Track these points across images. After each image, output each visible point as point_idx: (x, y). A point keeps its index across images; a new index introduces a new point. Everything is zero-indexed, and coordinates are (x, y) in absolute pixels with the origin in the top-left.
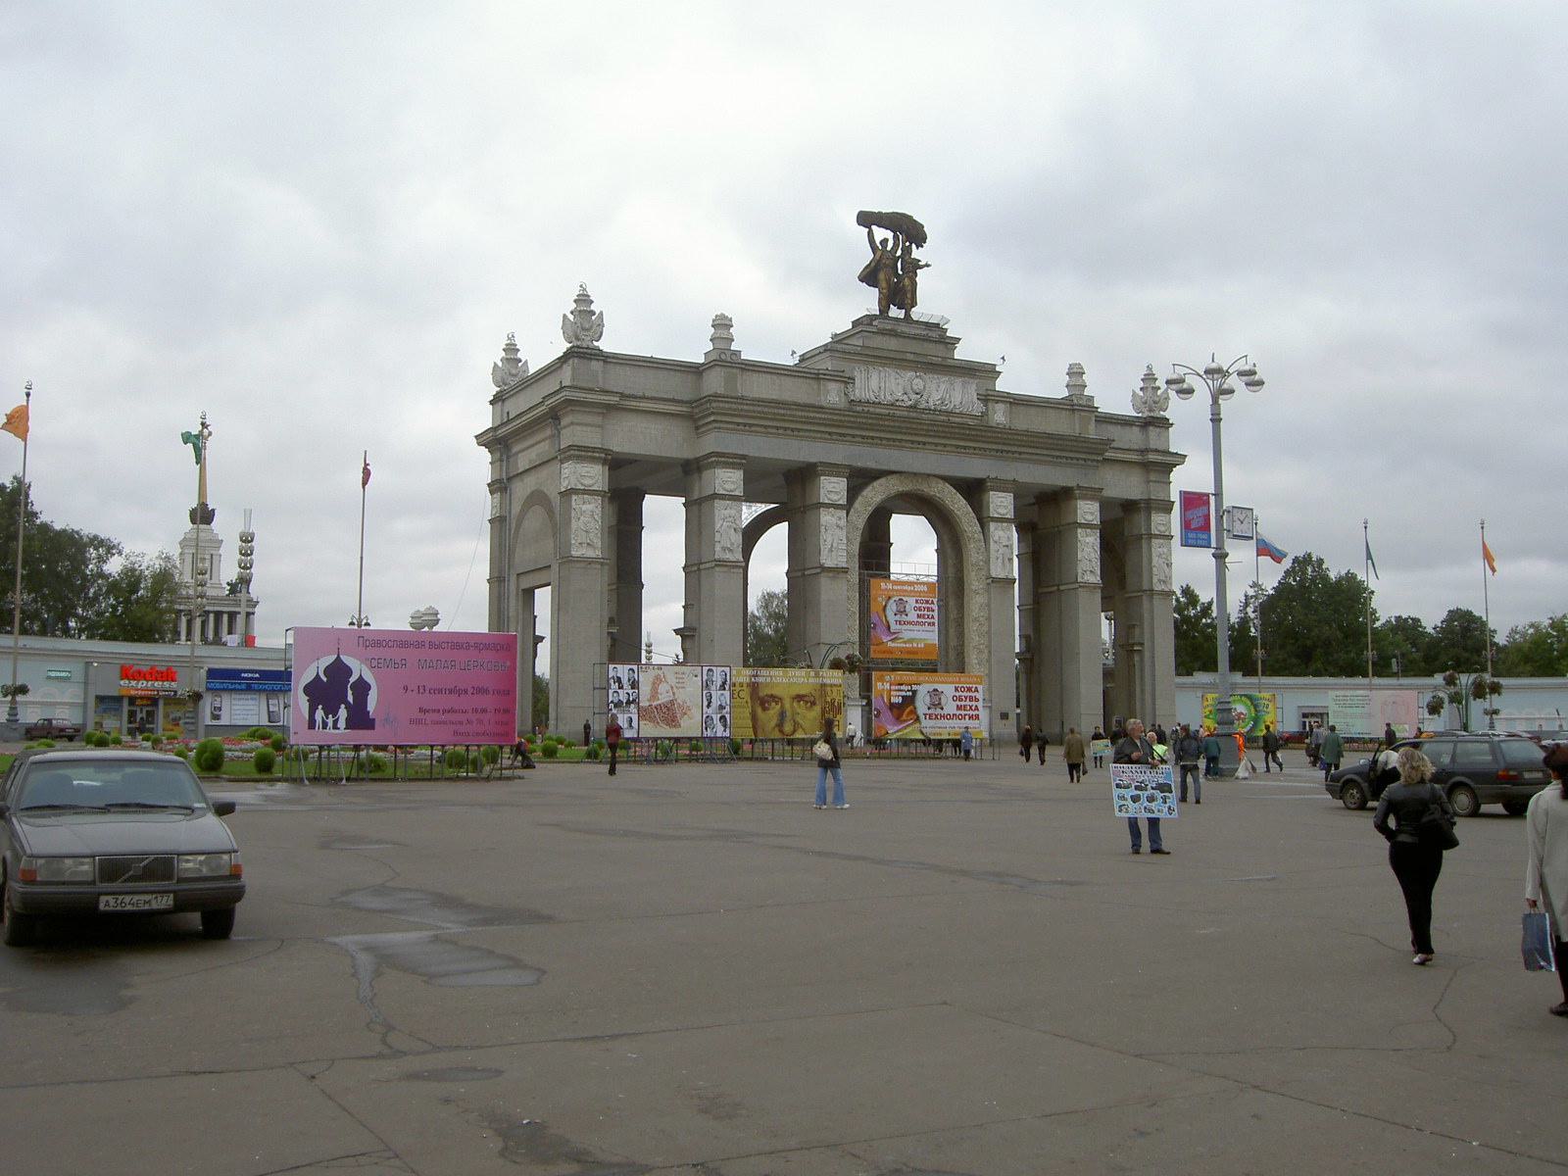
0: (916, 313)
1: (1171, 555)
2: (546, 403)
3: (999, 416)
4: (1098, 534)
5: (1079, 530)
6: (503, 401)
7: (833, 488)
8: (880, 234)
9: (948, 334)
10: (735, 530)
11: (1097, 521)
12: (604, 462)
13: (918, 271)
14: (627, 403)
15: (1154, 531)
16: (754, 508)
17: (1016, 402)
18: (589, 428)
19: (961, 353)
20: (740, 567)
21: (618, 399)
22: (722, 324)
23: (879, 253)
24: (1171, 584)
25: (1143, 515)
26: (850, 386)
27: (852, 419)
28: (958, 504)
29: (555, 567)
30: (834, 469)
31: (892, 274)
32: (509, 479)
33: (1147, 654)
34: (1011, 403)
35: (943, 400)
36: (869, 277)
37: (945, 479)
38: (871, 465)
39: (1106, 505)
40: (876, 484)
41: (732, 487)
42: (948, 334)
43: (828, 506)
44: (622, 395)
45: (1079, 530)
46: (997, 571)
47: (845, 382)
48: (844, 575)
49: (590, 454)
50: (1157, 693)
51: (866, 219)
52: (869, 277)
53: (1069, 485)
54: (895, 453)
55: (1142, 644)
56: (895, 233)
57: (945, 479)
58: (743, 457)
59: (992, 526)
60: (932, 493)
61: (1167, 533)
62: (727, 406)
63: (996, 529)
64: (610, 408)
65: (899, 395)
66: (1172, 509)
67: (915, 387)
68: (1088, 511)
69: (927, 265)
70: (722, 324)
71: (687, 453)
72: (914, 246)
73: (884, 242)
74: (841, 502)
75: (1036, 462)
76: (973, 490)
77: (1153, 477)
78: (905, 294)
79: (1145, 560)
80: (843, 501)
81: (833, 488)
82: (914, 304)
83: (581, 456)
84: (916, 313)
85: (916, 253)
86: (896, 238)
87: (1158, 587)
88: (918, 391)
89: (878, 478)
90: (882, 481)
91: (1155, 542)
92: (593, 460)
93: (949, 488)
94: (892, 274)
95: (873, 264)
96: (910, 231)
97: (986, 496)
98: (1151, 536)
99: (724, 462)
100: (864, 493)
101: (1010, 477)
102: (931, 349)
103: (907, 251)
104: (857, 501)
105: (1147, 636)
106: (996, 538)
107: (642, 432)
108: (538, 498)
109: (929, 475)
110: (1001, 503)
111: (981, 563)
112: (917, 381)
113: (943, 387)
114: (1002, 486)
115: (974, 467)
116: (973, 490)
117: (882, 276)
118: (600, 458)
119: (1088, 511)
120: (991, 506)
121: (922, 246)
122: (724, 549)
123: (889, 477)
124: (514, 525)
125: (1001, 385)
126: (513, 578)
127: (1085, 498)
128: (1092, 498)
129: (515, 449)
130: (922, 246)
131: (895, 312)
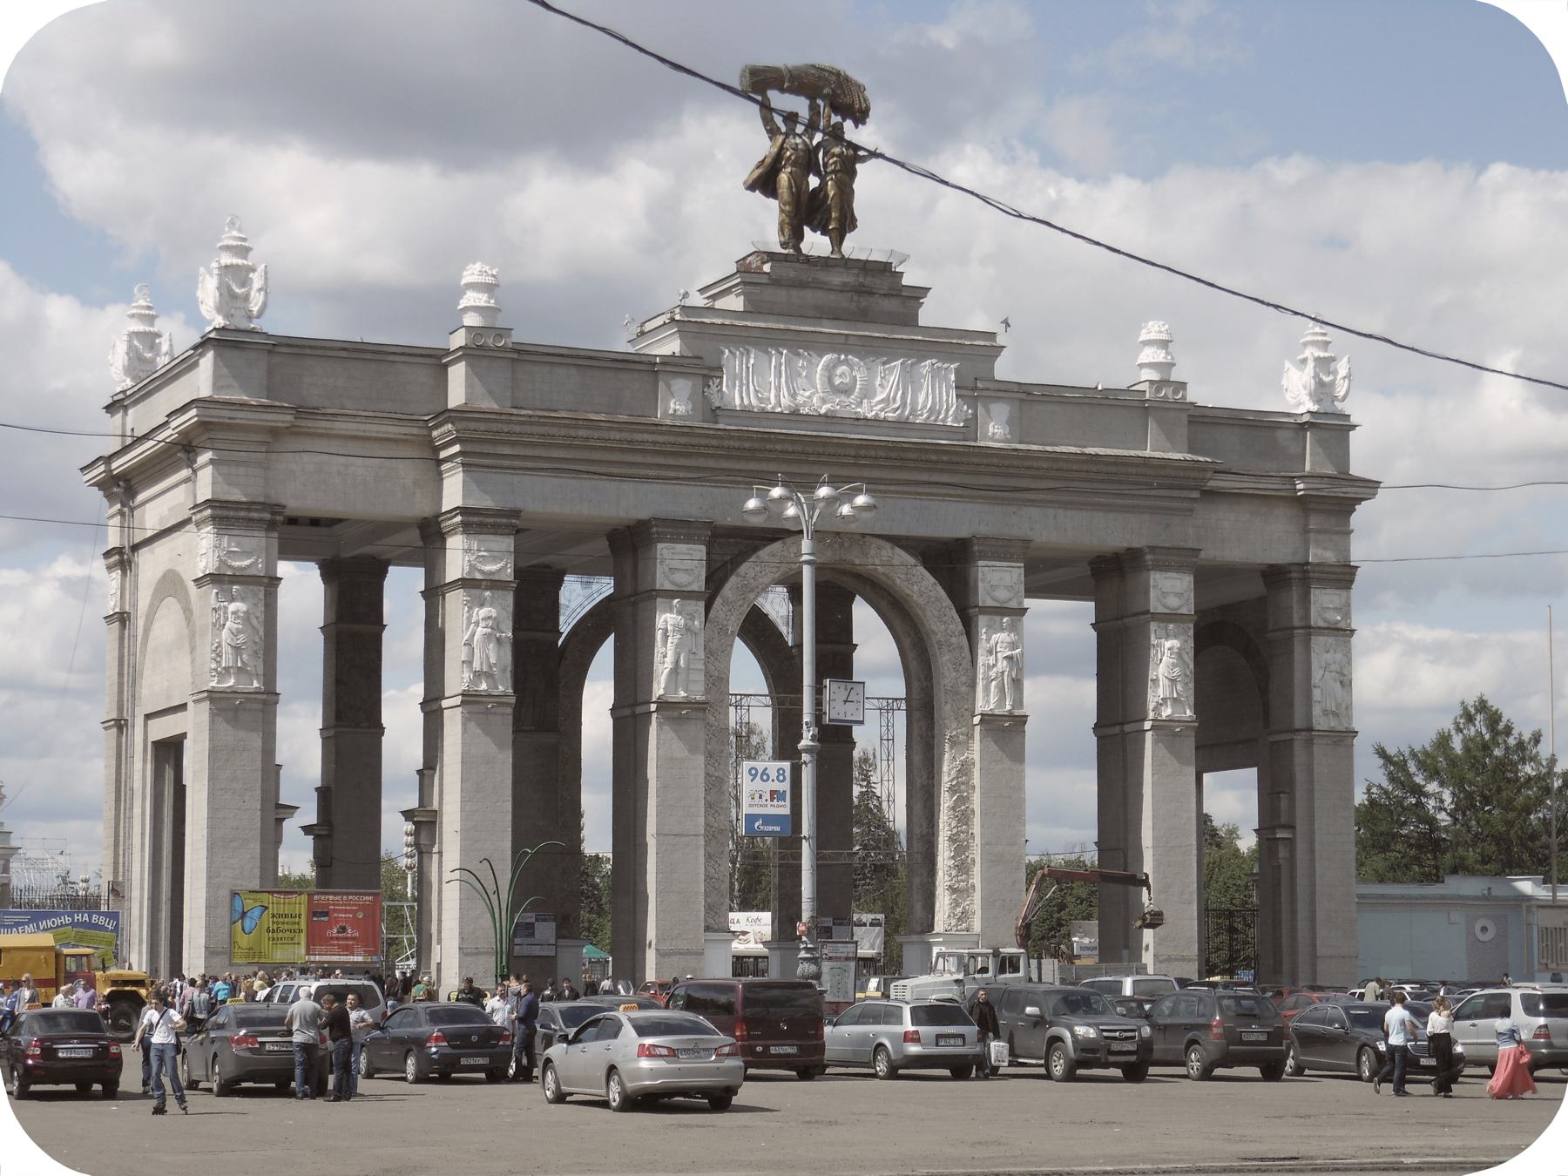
0: (852, 246)
1: (1349, 662)
2: (173, 425)
4: (1191, 633)
5: (1153, 626)
6: (126, 408)
7: (678, 563)
8: (782, 101)
9: (905, 282)
10: (499, 640)
11: (1188, 608)
12: (271, 526)
13: (858, 166)
14: (310, 423)
15: (1315, 620)
16: (595, 587)
17: (1029, 398)
18: (242, 470)
19: (930, 315)
20: (508, 704)
21: (290, 418)
24: (1350, 717)
25: (1295, 594)
27: (714, 442)
28: (922, 587)
29: (191, 705)
30: (681, 529)
32: (135, 548)
33: (1301, 846)
34: (1022, 400)
35: (886, 401)
36: (765, 182)
39: (1207, 576)
40: (764, 553)
41: (494, 567)
42: (905, 282)
43: (671, 595)
44: (300, 411)
48: (700, 715)
49: (242, 514)
50: (1320, 916)
51: (759, 84)
52: (765, 182)
53: (1135, 545)
55: (1292, 827)
56: (812, 99)
58: (515, 513)
59: (983, 621)
61: (1342, 625)
62: (482, 426)
64: (275, 433)
65: (800, 399)
66: (1352, 582)
67: (837, 381)
68: (1171, 590)
71: (421, 509)
72: (848, 125)
74: (695, 587)
75: (1067, 505)
76: (950, 561)
77: (1314, 522)
79: (1298, 675)
80: (699, 585)
81: (678, 563)
82: (847, 222)
83: (227, 518)
84: (852, 246)
85: (851, 132)
86: (814, 109)
87: (1320, 722)
89: (774, 540)
90: (777, 546)
91: (1318, 642)
92: (249, 523)
95: (768, 161)
96: (838, 97)
97: (972, 570)
98: (1309, 629)
99: (481, 525)
100: (743, 569)
102: (875, 304)
103: (836, 134)
104: (729, 590)
105: (1300, 812)
107: (339, 473)
108: (170, 584)
109: (863, 535)
110: (996, 580)
111: (963, 689)
114: (1003, 549)
115: (951, 519)
116: (950, 561)
117: (783, 178)
118: (261, 520)
119: (1171, 590)
120: (980, 585)
121: (864, 123)
122: (478, 675)
124: (140, 631)
125: (1004, 369)
126: (139, 721)
127: (1164, 567)
128: (1179, 568)
129: (141, 497)
131: (815, 243)
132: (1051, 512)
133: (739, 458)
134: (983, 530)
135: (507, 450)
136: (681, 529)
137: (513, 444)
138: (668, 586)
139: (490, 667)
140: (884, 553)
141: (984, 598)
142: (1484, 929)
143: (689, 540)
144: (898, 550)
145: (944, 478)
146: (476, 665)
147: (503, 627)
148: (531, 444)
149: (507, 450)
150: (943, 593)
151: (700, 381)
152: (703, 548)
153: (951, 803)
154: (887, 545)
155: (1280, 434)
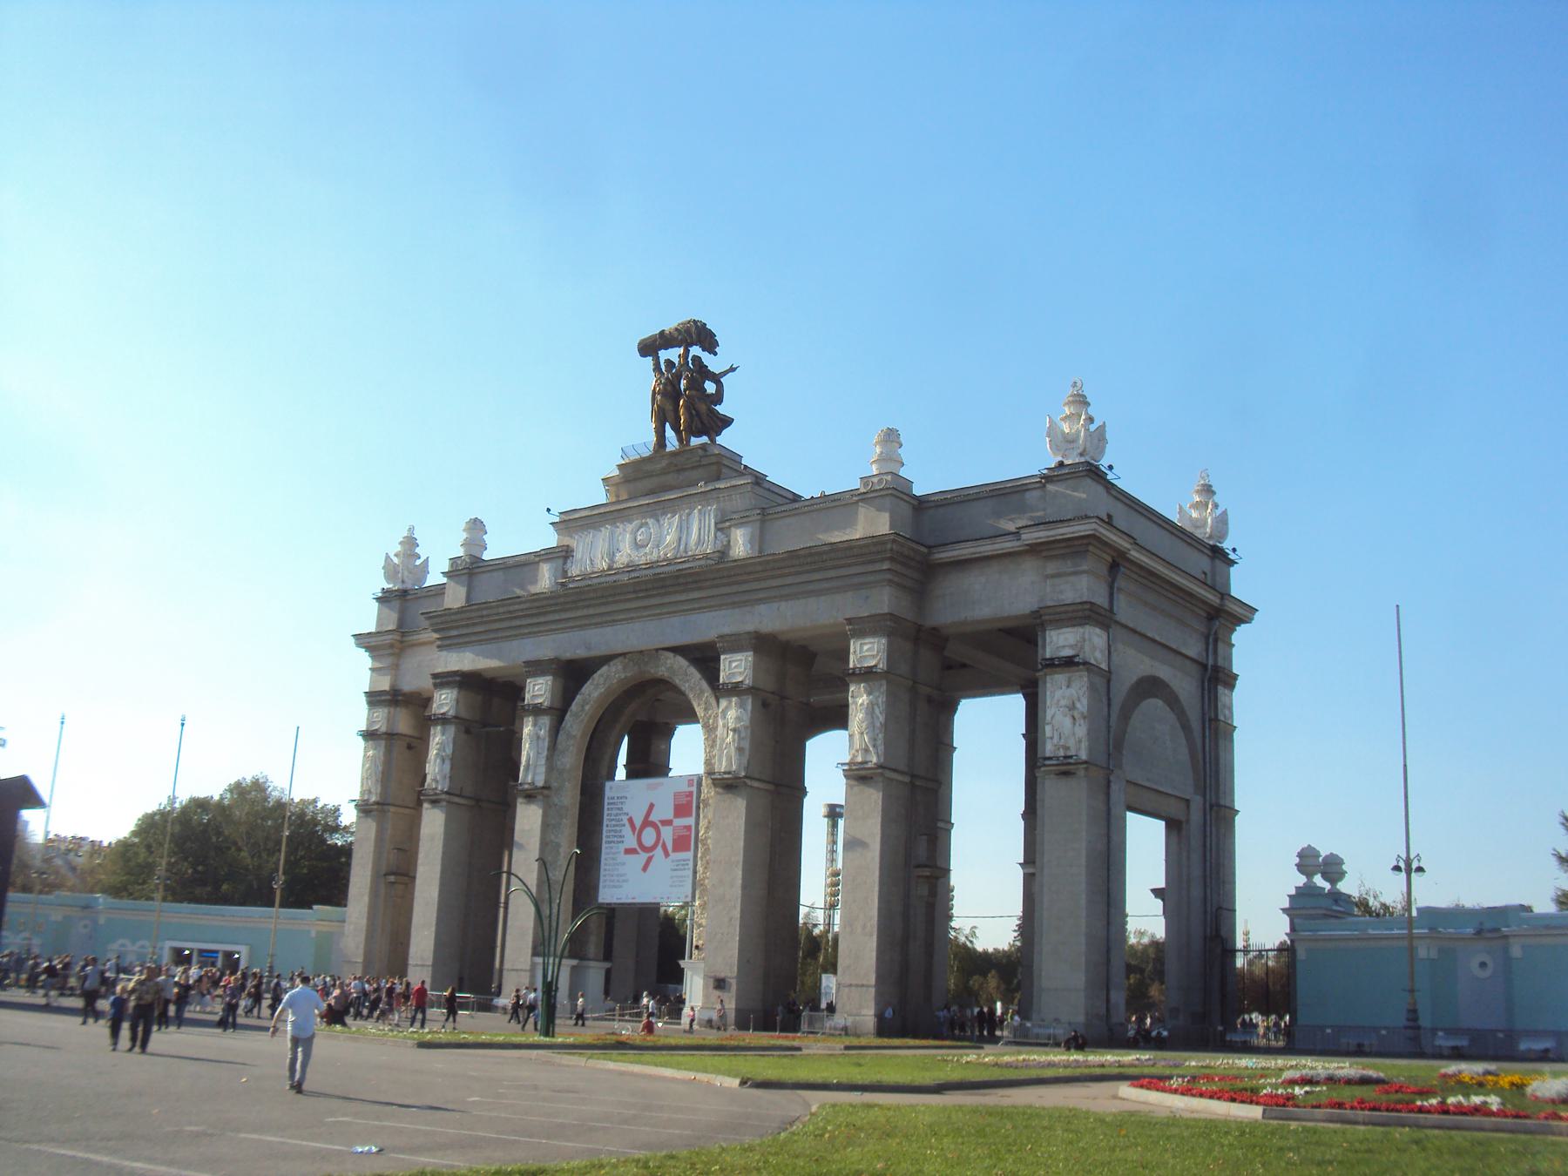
3: (741, 544)
8: (664, 355)
22: (476, 526)
31: (689, 398)
37: (675, 650)
38: (581, 653)
54: (608, 631)
57: (675, 650)
69: (732, 369)
70: (476, 526)
77: (1052, 567)
81: (539, 690)
85: (707, 358)
90: (604, 669)
93: (681, 662)
94: (689, 398)
101: (750, 627)
104: (574, 707)
110: (736, 667)
114: (735, 644)
132: (775, 605)
133: (571, 609)
134: (726, 630)
135: (454, 633)
136: (536, 668)
137: (457, 628)
142: (1483, 965)
143: (543, 674)
145: (696, 595)
148: (467, 626)
149: (454, 633)
150: (704, 685)
151: (560, 561)
154: (671, 655)
155: (1028, 495)
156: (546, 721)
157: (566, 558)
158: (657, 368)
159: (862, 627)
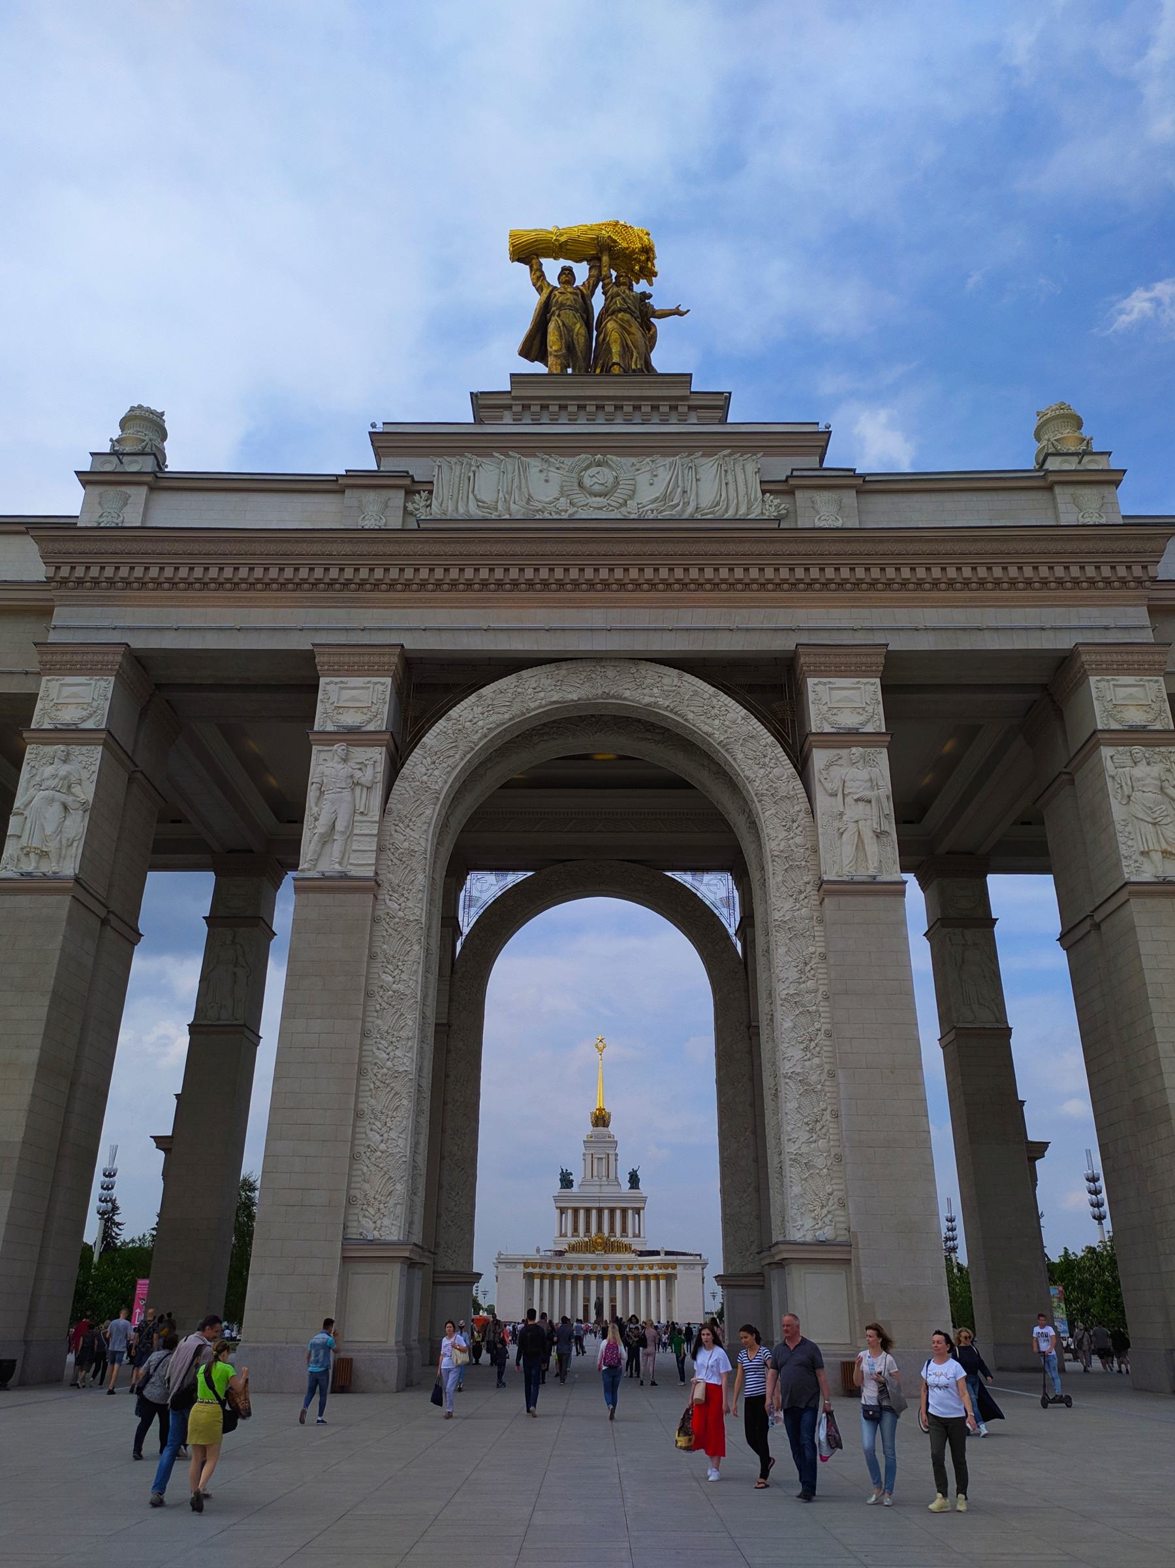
7: (355, 700)
10: (65, 807)
23: (546, 292)
26: (420, 500)
30: (356, 660)
35: (665, 498)
40: (487, 691)
43: (330, 738)
45: (1106, 752)
46: (839, 862)
47: (409, 493)
51: (528, 252)
59: (819, 758)
60: (647, 700)
63: (830, 764)
67: (587, 482)
69: (677, 312)
73: (567, 273)
78: (609, 351)
88: (597, 488)
100: (454, 713)
104: (429, 739)
106: (836, 785)
110: (843, 702)
112: (593, 470)
113: (664, 476)
114: (843, 660)
116: (770, 687)
117: (551, 326)
121: (655, 275)
123: (524, 673)
130: (655, 275)
138: (330, 728)
139: (45, 840)
140: (666, 681)
141: (816, 723)
144: (688, 677)
146: (24, 841)
147: (76, 790)
151: (401, 494)
152: (388, 681)
153: (788, 1024)
156: (377, 756)
157: (409, 493)
158: (539, 279)
159: (1126, 659)
